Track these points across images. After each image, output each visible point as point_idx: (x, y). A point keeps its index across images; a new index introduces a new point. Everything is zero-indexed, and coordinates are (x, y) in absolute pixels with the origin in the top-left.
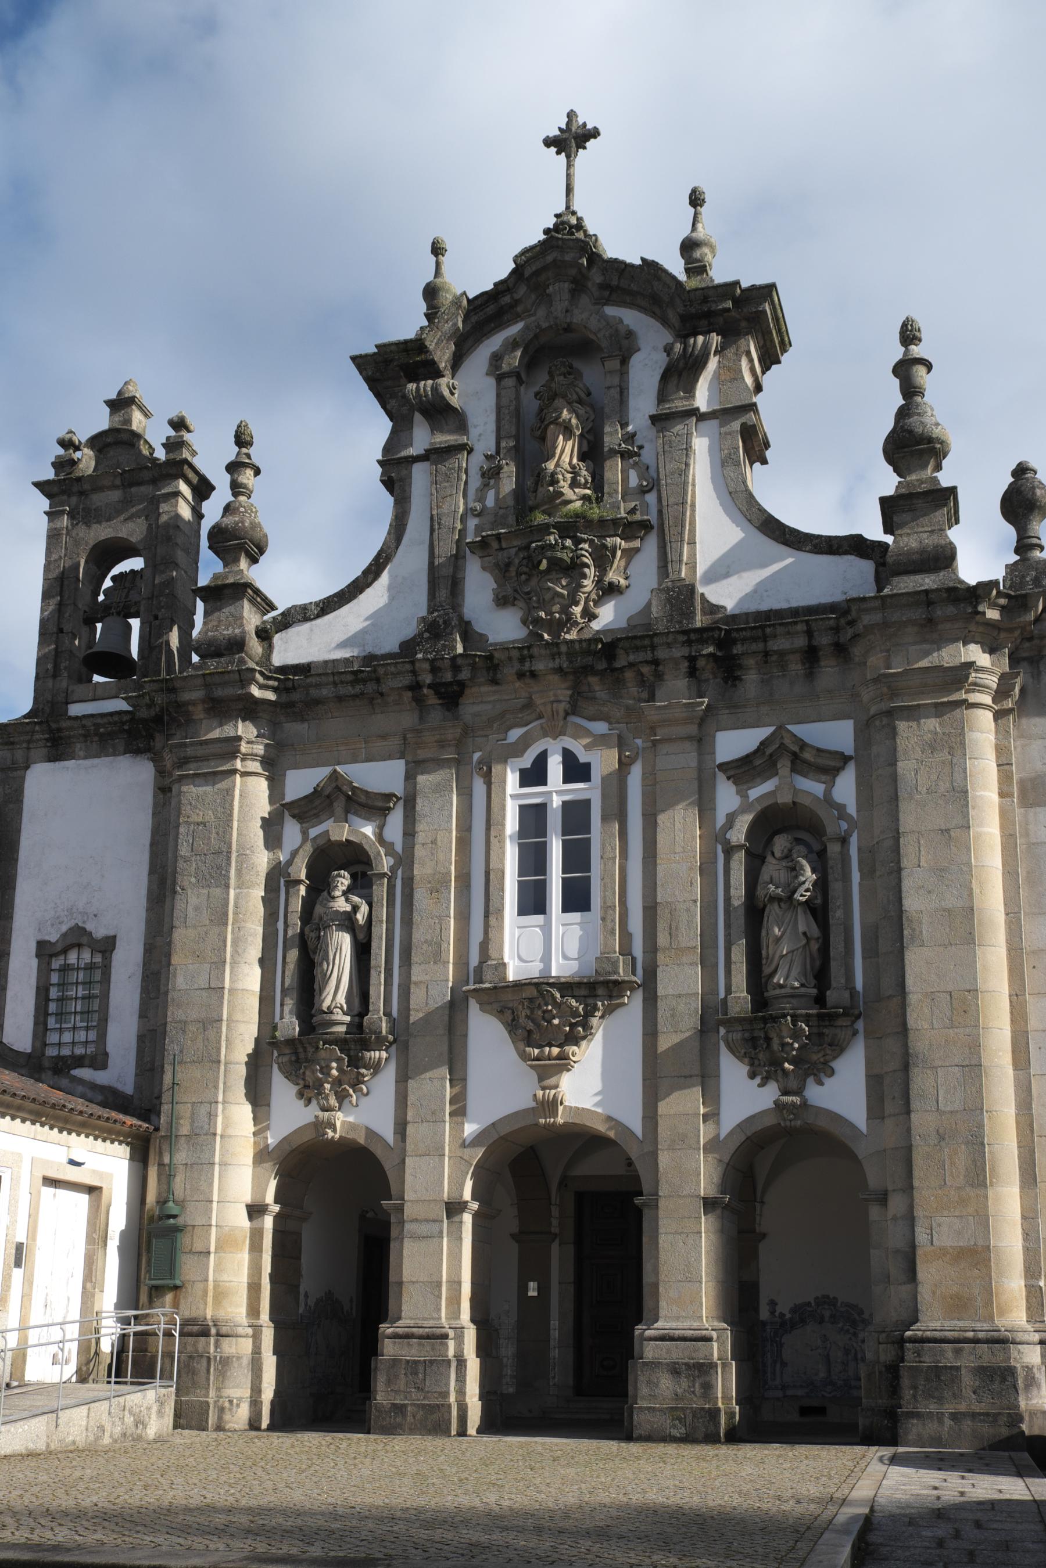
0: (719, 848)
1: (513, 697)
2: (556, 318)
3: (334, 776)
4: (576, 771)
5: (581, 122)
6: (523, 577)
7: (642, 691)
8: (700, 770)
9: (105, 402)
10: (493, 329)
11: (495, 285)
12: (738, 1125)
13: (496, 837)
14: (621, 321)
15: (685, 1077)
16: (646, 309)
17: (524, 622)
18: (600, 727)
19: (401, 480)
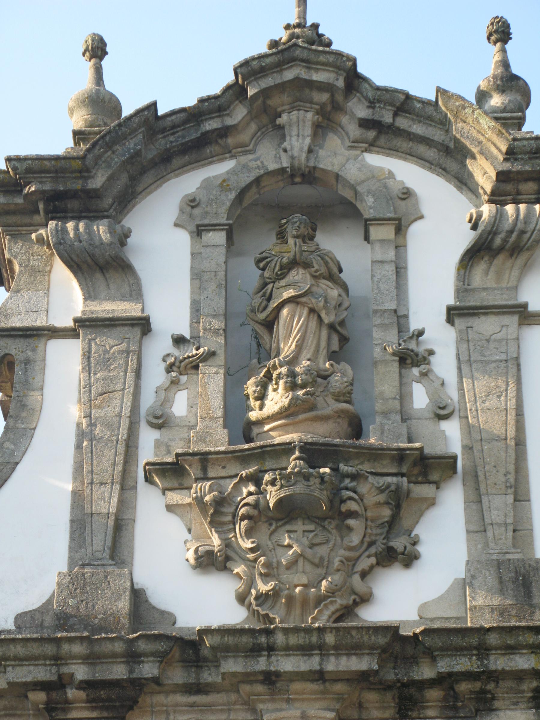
2: (292, 157)
10: (190, 163)
11: (202, 101)
14: (391, 175)
17: (242, 598)
19: (27, 362)
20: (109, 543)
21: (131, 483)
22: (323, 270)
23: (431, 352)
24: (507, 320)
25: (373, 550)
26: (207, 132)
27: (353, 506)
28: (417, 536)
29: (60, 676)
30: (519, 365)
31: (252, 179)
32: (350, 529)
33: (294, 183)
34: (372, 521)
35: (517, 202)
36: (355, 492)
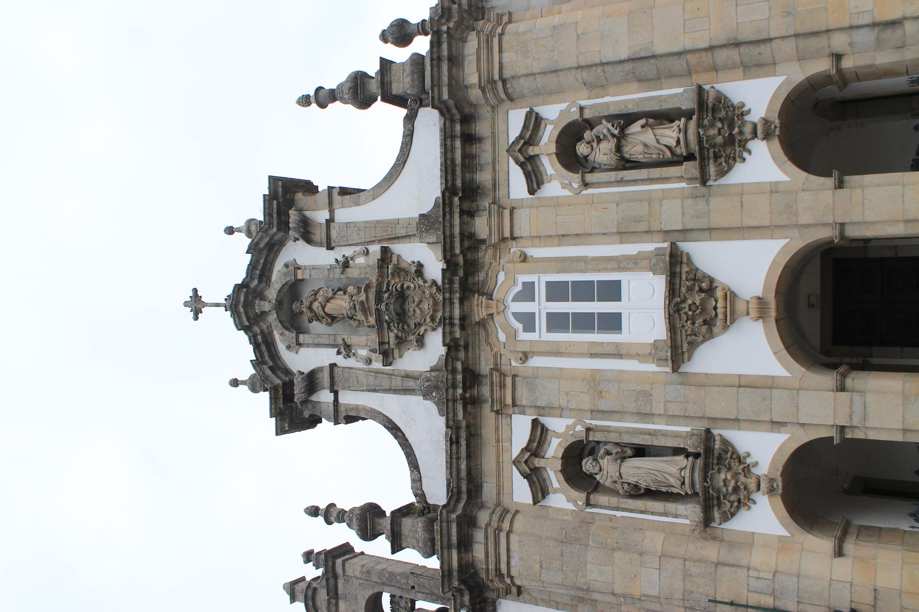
0: (584, 192)
1: (477, 336)
3: (516, 462)
4: (528, 293)
5: (190, 299)
6: (406, 327)
7: (481, 249)
8: (531, 207)
9: (291, 603)
11: (251, 344)
12: (779, 167)
13: (566, 349)
14: (279, 271)
15: (742, 206)
16: (275, 256)
17: (434, 329)
18: (501, 277)
20: (413, 380)
21: (391, 372)
22: (313, 297)
23: (344, 256)
24: (332, 228)
25: (416, 279)
26: (262, 341)
27: (399, 286)
28: (411, 262)
29: (461, 399)
30: (349, 223)
31: (279, 324)
32: (408, 287)
33: (282, 308)
34: (405, 279)
35: (289, 223)
36: (394, 285)
